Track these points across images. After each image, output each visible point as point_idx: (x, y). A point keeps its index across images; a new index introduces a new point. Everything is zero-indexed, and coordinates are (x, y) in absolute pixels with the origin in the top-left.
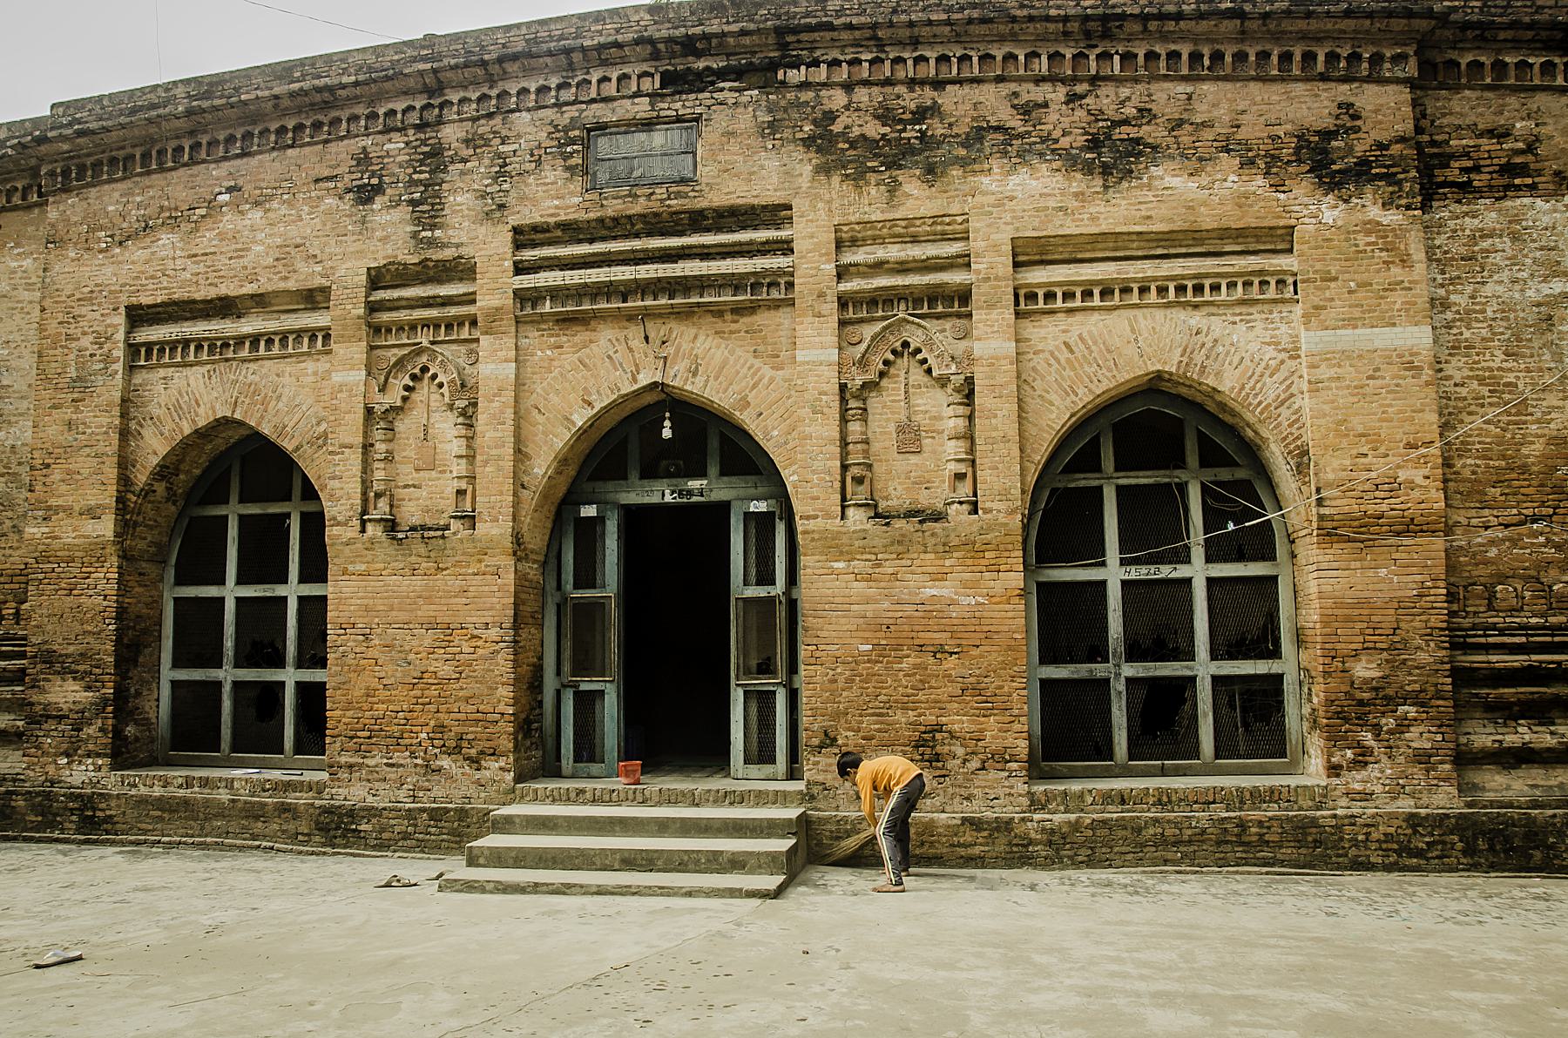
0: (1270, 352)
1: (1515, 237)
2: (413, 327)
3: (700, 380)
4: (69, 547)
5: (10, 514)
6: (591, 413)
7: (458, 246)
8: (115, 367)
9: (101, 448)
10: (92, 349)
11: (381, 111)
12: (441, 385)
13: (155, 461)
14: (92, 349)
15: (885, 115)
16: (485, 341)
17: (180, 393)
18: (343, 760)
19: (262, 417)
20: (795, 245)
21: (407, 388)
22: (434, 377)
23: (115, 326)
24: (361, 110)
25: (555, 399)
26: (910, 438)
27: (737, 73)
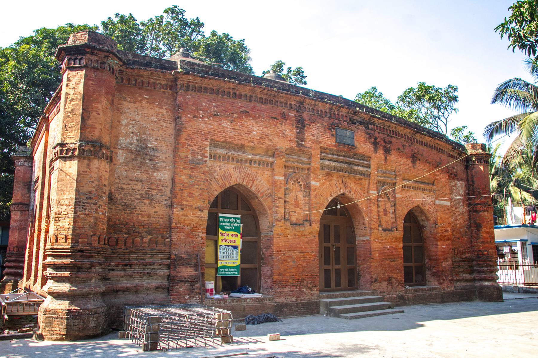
0: (431, 203)
1: (456, 187)
2: (294, 167)
3: (352, 193)
4: (191, 220)
5: (158, 205)
6: (332, 198)
7: (309, 148)
8: (205, 159)
9: (202, 187)
10: (197, 151)
11: (288, 104)
12: (301, 185)
13: (216, 193)
14: (197, 151)
15: (384, 141)
16: (312, 175)
17: (225, 172)
18: (278, 290)
19: (252, 185)
20: (372, 166)
21: (293, 184)
22: (299, 182)
23: (207, 145)
24: (282, 100)
25: (325, 193)
26: (386, 213)
27: (361, 123)
